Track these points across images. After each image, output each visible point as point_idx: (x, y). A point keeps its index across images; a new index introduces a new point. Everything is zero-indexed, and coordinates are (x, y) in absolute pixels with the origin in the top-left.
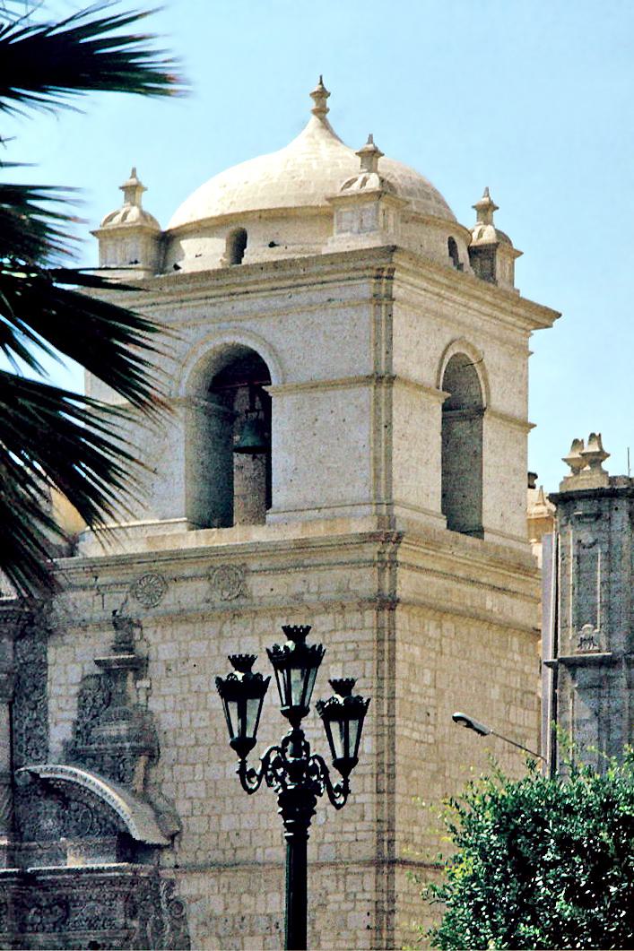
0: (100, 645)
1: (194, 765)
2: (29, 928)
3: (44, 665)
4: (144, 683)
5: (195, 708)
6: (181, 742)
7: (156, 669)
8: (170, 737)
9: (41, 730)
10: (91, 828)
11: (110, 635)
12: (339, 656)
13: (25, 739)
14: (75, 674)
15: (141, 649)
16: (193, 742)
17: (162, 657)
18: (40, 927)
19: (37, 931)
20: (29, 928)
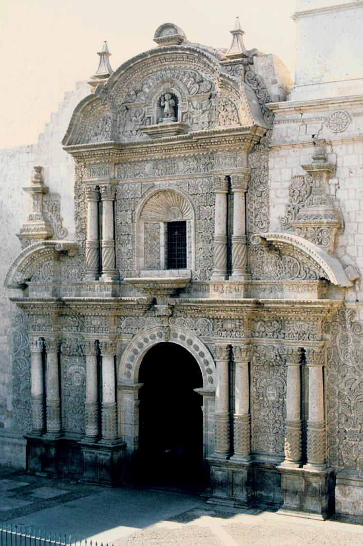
0: (307, 155)
2: (257, 334)
3: (266, 169)
4: (333, 181)
7: (342, 172)
8: (352, 215)
9: (265, 210)
10: (300, 273)
11: (311, 151)
13: (254, 215)
14: (287, 175)
15: (332, 159)
17: (346, 164)
18: (264, 334)
19: (262, 337)
20: (257, 334)
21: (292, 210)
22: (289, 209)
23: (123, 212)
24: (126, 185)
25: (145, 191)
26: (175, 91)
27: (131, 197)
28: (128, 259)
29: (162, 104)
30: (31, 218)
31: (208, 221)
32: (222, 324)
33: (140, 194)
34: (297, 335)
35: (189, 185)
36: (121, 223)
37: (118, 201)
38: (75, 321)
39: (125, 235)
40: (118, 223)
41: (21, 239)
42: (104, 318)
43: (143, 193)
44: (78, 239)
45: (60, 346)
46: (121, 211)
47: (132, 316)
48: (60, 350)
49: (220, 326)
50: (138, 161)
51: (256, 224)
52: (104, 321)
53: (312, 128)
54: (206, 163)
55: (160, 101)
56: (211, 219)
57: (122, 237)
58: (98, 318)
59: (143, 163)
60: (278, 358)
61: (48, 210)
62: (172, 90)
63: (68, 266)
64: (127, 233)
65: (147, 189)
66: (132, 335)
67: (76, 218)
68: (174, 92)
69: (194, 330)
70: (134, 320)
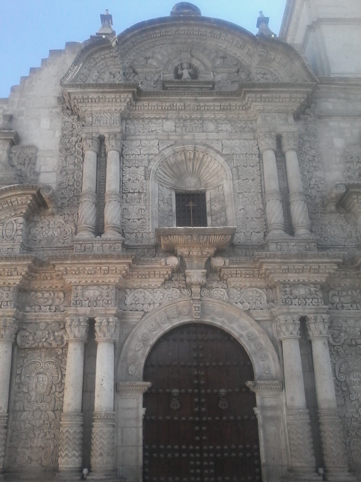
14: (339, 143)
21: (352, 175)
23: (132, 168)
24: (137, 141)
25: (163, 148)
26: (196, 63)
27: (145, 153)
28: (139, 220)
29: (180, 72)
31: (250, 181)
32: (291, 291)
33: (157, 150)
35: (222, 145)
36: (129, 180)
37: (125, 156)
38: (47, 298)
39: (134, 193)
40: (125, 179)
42: (105, 287)
44: (62, 196)
45: (16, 334)
46: (130, 167)
48: (16, 339)
50: (154, 118)
51: (311, 186)
52: (104, 291)
54: (242, 126)
55: (176, 70)
56: (253, 180)
57: (129, 195)
58: (95, 287)
59: (161, 121)
61: (18, 163)
63: (42, 228)
64: (137, 191)
65: (166, 146)
66: (143, 313)
69: (239, 304)
70: (147, 293)
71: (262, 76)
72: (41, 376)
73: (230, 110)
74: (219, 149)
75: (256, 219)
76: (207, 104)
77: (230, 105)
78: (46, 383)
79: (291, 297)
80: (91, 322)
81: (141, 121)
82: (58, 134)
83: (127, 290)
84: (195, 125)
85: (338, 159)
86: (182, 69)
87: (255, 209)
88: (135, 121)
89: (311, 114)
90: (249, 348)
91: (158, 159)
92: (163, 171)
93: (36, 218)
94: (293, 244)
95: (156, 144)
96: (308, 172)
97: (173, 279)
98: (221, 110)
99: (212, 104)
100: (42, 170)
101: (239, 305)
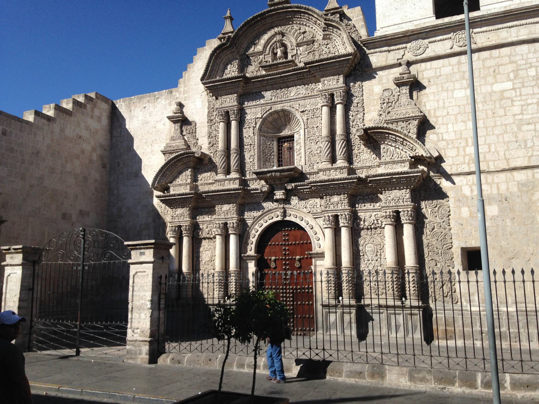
1: (447, 124)
5: (446, 98)
6: (438, 113)
10: (393, 156)
12: (533, 64)
16: (445, 113)
17: (425, 76)
21: (383, 113)
22: (381, 113)
30: (173, 139)
31: (315, 129)
34: (394, 201)
41: (164, 154)
43: (262, 114)
44: (210, 151)
47: (254, 203)
49: (328, 201)
53: (397, 54)
56: (317, 127)
58: (227, 205)
60: (375, 222)
62: (282, 40)
67: (209, 137)
68: (284, 42)
70: (256, 206)
71: (325, 46)
72: (207, 252)
73: (304, 78)
74: (297, 108)
75: (317, 154)
76: (289, 78)
77: (303, 76)
78: (209, 256)
79: (329, 203)
80: (226, 224)
81: (251, 95)
82: (206, 111)
83: (245, 205)
84: (284, 93)
85: (375, 102)
86: (277, 48)
87: (317, 147)
88: (248, 96)
89: (360, 69)
90: (310, 233)
91: (261, 120)
92: (266, 127)
93: (198, 167)
94: (333, 171)
95: (260, 110)
96: (353, 116)
97: (269, 197)
98: (298, 79)
99: (292, 77)
100: (200, 136)
101: (305, 210)
